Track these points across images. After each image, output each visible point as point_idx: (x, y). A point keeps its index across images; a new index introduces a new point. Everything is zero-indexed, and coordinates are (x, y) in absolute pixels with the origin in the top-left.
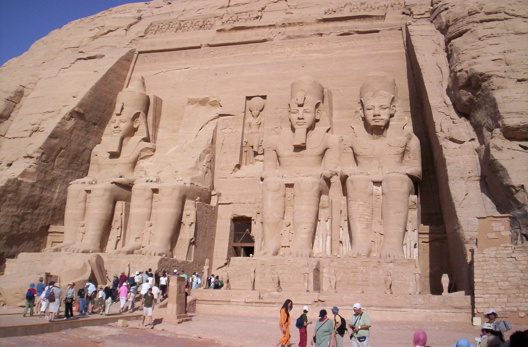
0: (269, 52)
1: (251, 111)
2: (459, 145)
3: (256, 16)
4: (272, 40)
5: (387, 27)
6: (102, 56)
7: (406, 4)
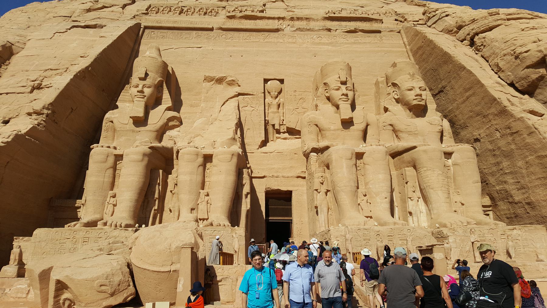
1: (269, 93)
2: (540, 118)
3: (261, 9)
4: (283, 30)
6: (102, 27)
7: (399, 13)
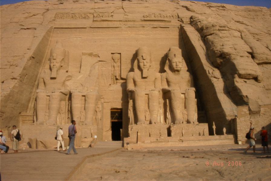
0: (120, 33)
2: (217, 80)
3: (111, 15)
5: (172, 26)
7: (179, 17)
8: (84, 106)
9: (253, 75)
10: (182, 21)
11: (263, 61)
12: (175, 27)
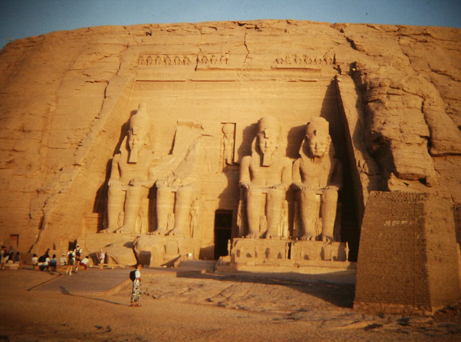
1: (225, 134)
7: (336, 61)
8: (173, 206)
9: (418, 175)
10: (339, 71)
11: (445, 152)
12: (325, 81)
